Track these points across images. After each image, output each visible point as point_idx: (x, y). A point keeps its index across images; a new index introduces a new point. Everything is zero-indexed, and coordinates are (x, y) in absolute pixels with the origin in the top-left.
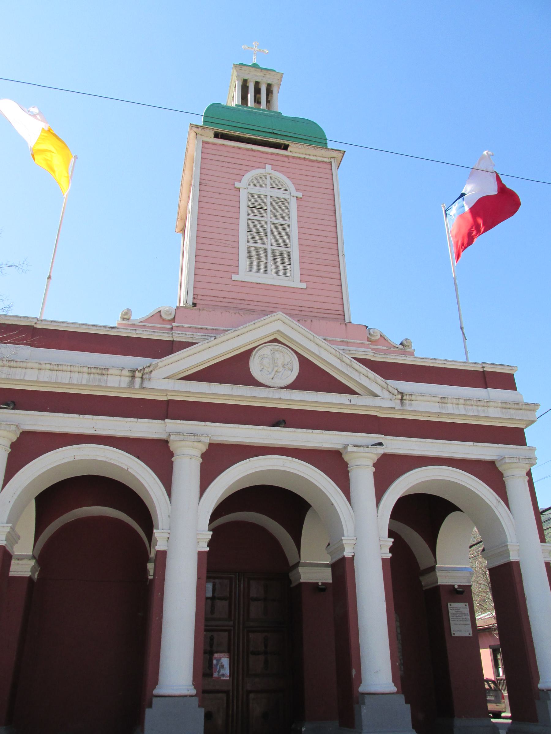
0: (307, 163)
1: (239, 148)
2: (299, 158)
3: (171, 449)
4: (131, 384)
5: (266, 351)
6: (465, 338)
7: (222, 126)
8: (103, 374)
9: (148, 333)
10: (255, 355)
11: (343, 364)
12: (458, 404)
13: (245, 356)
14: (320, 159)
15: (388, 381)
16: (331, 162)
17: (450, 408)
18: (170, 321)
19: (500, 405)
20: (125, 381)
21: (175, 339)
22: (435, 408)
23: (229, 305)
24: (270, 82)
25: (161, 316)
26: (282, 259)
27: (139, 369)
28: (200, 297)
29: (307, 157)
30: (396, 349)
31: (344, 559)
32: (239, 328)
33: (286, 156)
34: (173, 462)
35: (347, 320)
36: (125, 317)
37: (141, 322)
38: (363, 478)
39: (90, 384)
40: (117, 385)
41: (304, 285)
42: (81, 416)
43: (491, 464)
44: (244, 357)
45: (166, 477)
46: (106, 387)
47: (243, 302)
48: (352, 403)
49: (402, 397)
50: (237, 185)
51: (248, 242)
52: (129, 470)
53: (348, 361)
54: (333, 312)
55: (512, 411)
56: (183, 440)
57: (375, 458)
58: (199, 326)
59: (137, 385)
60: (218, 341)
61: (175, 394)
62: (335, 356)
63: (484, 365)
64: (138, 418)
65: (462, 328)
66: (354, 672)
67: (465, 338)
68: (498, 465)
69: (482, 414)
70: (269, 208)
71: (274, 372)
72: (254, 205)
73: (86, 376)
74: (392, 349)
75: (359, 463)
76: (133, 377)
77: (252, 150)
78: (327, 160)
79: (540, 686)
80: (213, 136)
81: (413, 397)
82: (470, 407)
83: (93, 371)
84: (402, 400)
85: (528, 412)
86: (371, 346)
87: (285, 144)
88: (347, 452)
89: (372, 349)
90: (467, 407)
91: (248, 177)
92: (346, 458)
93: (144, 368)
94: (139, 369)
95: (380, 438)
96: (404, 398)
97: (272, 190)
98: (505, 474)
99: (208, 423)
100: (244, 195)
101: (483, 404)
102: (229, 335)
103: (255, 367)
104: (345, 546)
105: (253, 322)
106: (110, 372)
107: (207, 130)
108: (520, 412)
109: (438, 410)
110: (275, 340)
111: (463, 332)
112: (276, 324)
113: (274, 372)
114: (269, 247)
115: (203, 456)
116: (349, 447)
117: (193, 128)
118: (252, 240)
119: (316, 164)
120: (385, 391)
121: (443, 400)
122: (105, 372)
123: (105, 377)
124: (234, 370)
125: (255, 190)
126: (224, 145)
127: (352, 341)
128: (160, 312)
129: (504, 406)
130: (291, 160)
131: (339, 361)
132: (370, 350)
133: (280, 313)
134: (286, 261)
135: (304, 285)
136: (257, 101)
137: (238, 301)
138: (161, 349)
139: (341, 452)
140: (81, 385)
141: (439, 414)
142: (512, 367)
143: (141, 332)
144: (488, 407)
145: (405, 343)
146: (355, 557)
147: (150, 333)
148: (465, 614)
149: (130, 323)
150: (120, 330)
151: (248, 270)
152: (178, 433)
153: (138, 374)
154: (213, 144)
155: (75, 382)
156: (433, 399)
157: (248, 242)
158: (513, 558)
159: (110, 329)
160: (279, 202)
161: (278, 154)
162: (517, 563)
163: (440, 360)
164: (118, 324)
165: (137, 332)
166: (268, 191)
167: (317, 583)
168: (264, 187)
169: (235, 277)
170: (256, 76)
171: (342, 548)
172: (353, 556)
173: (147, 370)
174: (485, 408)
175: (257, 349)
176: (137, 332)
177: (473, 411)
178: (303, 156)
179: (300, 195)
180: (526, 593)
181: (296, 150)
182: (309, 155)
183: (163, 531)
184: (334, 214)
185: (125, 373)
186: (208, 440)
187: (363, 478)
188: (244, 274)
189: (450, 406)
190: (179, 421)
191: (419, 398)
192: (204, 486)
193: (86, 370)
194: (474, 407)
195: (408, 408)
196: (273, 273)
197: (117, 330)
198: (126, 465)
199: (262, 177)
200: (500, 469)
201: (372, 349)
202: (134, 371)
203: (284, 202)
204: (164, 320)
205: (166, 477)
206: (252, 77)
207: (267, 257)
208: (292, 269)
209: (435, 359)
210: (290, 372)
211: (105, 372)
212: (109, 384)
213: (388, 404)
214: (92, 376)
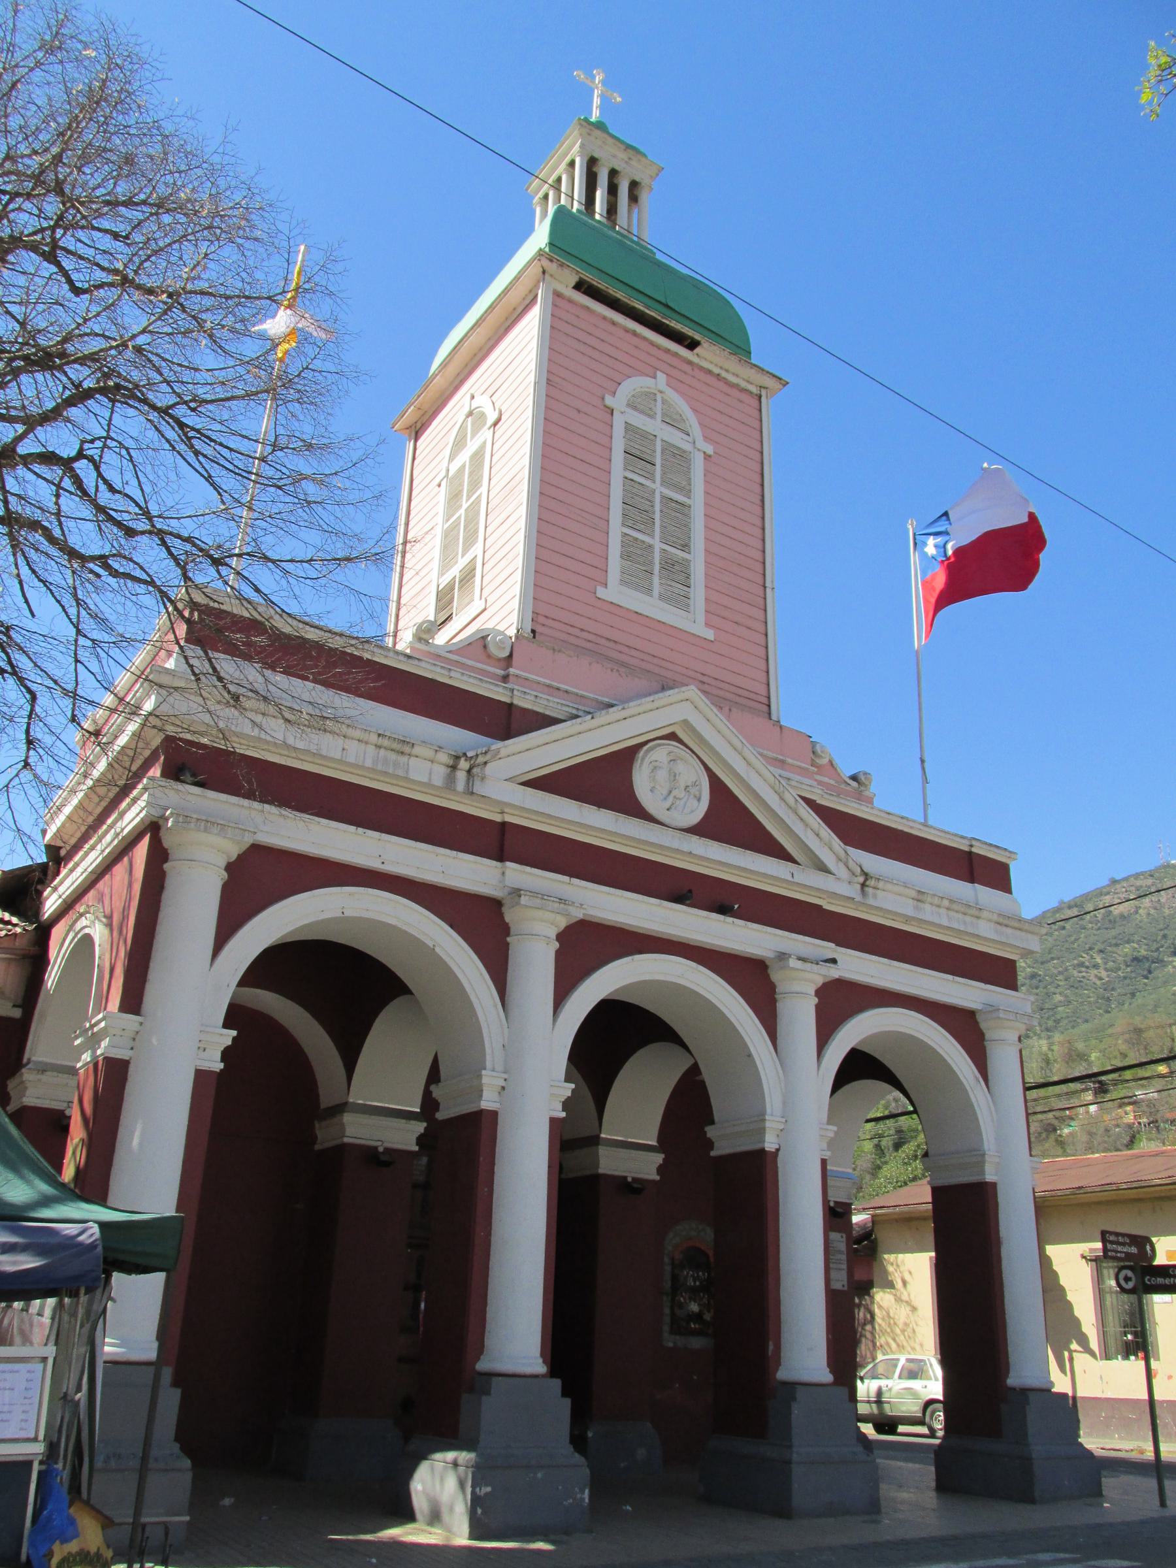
0: (721, 385)
1: (614, 323)
2: (710, 372)
3: (507, 919)
4: (450, 780)
5: (661, 754)
6: (925, 780)
7: (630, 291)
8: (402, 753)
9: (471, 680)
10: (643, 759)
11: (783, 804)
12: (939, 906)
14: (743, 384)
15: (850, 850)
16: (760, 397)
17: (928, 912)
18: (499, 660)
19: (995, 917)
20: (439, 774)
21: (515, 702)
22: (906, 907)
23: (589, 645)
24: (596, 156)
25: (485, 647)
26: (676, 571)
27: (470, 754)
28: (541, 619)
29: (724, 374)
30: (848, 788)
31: (762, 1152)
32: (631, 704)
33: (690, 363)
34: (508, 944)
35: (774, 717)
36: (424, 636)
37: (450, 652)
38: (800, 1013)
39: (380, 767)
40: (425, 780)
41: (709, 634)
42: (361, 830)
43: (970, 1015)
44: (623, 760)
46: (407, 779)
47: (611, 645)
48: (796, 879)
49: (866, 880)
50: (609, 401)
51: (623, 525)
52: (437, 950)
53: (791, 801)
54: (752, 696)
55: (1009, 931)
56: (541, 909)
57: (820, 981)
58: (555, 684)
59: (460, 785)
60: (595, 723)
61: (516, 813)
62: (773, 788)
63: (974, 843)
64: (382, 831)
65: (922, 761)
66: (771, 1347)
67: (925, 780)
68: (979, 1018)
69: (970, 930)
70: (658, 462)
72: (633, 451)
73: (371, 749)
74: (843, 786)
75: (798, 989)
76: (454, 768)
77: (635, 334)
78: (754, 390)
79: (1012, 1381)
80: (573, 284)
81: (881, 885)
82: (955, 914)
83: (386, 742)
84: (863, 885)
85: (1029, 936)
86: (818, 777)
87: (693, 339)
88: (786, 967)
89: (820, 783)
90: (951, 913)
92: (775, 976)
93: (477, 755)
94: (470, 754)
95: (828, 948)
96: (868, 883)
97: (664, 426)
98: (988, 1035)
99: (575, 881)
101: (973, 912)
102: (614, 714)
104: (767, 1131)
105: (651, 698)
106: (417, 750)
107: (566, 271)
108: (1018, 933)
109: (910, 912)
110: (672, 736)
111: (923, 769)
112: (681, 707)
114: (658, 545)
115: (560, 937)
116: (791, 960)
117: (543, 259)
118: (630, 523)
119: (735, 393)
120: (841, 865)
121: (920, 897)
122: (407, 749)
123: (405, 759)
125: (638, 420)
126: (588, 308)
127: (790, 761)
128: (484, 638)
129: (1001, 920)
130: (697, 373)
131: (776, 797)
132: (815, 783)
133: (692, 687)
134: (681, 578)
135: (709, 634)
136: (612, 210)
137: (603, 641)
138: (505, 721)
139: (768, 963)
140: (362, 767)
141: (908, 919)
142: (1011, 852)
143: (458, 676)
144: (978, 918)
145: (862, 778)
146: (780, 1153)
147: (475, 682)
148: (840, 1252)
149: (432, 650)
150: (423, 664)
151: (623, 582)
152: (534, 894)
153: (464, 765)
154: (570, 301)
155: (351, 759)
156: (907, 891)
157: (623, 525)
158: (989, 1177)
159: (405, 659)
160: (674, 455)
161: (676, 355)
162: (994, 1185)
163: (914, 821)
164: (412, 648)
165: (453, 674)
167: (625, 1178)
168: (649, 416)
169: (601, 592)
170: (614, 156)
171: (762, 1131)
172: (778, 1150)
173: (481, 759)
174: (975, 920)
175: (645, 748)
176: (453, 674)
177: (957, 921)
178: (716, 370)
179: (710, 450)
180: (1003, 1232)
181: (709, 355)
182: (727, 371)
183: (494, 1074)
184: (759, 502)
185: (443, 758)
186: (578, 915)
187: (800, 1013)
188: (614, 591)
189: (927, 907)
190: (528, 869)
191: (889, 887)
193: (373, 738)
194: (960, 916)
195: (871, 901)
196: (661, 597)
197: (416, 662)
198: (432, 939)
199: (650, 394)
200: (983, 1026)
201: (820, 783)
202: (457, 758)
204: (489, 656)
206: (610, 158)
207: (652, 563)
208: (692, 596)
209: (907, 819)
210: (695, 803)
211: (407, 749)
212: (412, 776)
213: (844, 889)
214: (382, 751)
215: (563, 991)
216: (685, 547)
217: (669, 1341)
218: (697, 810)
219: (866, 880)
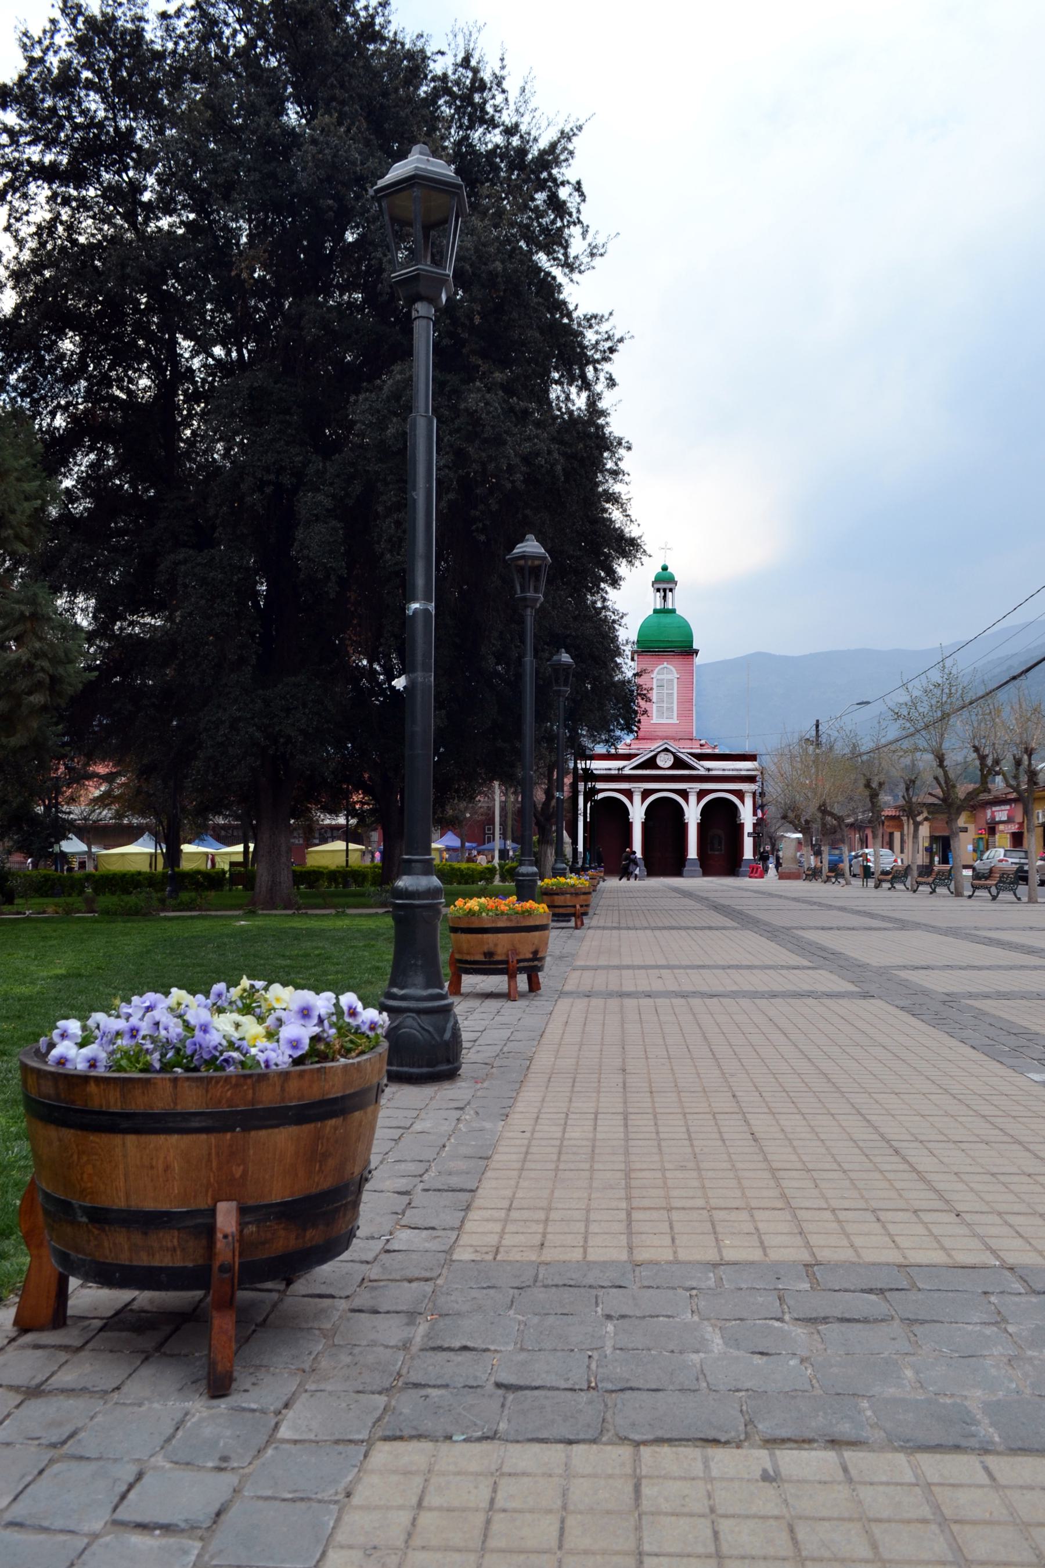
5: (662, 754)
13: (654, 757)
44: (654, 757)
71: (665, 761)
103: (660, 762)
113: (665, 761)
124: (651, 763)
125: (660, 677)
166: (665, 677)
203: (672, 680)
215: (643, 801)
218: (670, 763)
219: (709, 770)
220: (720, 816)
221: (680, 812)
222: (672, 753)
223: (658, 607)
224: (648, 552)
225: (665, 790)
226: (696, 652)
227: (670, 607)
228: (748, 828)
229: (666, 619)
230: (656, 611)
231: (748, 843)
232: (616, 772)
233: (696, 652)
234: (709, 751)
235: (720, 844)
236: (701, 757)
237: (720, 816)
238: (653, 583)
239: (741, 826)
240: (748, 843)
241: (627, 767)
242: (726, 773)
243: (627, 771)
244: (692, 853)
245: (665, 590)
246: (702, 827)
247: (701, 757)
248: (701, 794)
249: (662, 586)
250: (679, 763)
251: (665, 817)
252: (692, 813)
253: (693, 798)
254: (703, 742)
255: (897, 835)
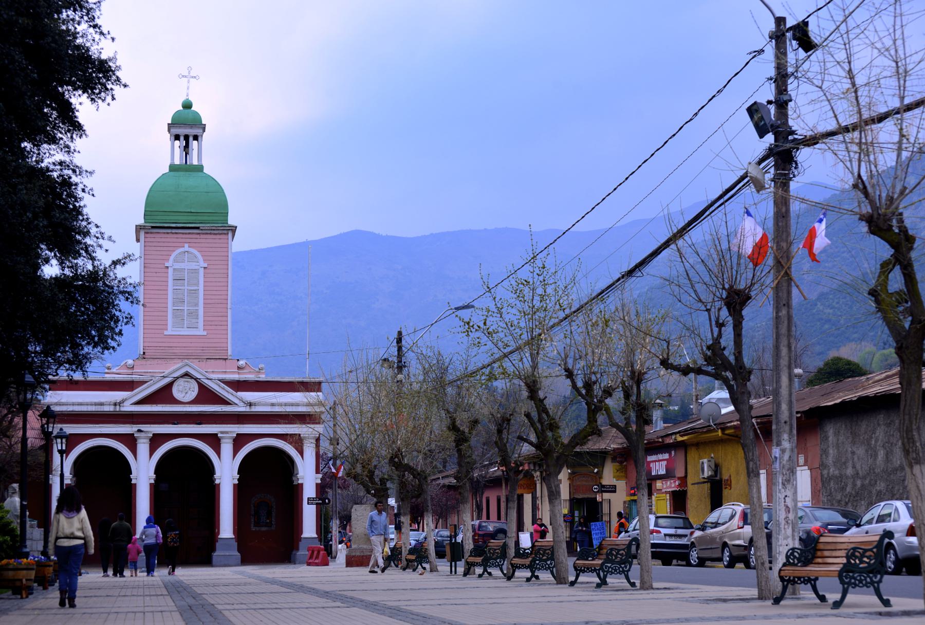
5: (181, 382)
13: (169, 386)
44: (169, 386)
45: (134, 451)
71: (185, 392)
91: (172, 258)
100: (170, 270)
113: (185, 392)
114: (186, 308)
124: (164, 394)
125: (177, 266)
162: (302, 484)
169: (166, 333)
192: (151, 454)
205: (134, 451)
215: (152, 452)
216: (197, 305)
217: (273, 528)
219: (250, 405)
220: (268, 473)
221: (209, 469)
222: (196, 379)
223: (177, 162)
224: (123, 81)
225: (185, 436)
226: (233, 229)
227: (195, 162)
228: (309, 491)
229: (188, 181)
230: (173, 168)
231: (309, 514)
232: (111, 408)
233: (233, 229)
234: (251, 377)
235: (269, 515)
236: (239, 386)
237: (268, 473)
238: (170, 126)
239: (298, 489)
240: (309, 514)
241: (128, 401)
242: (277, 409)
243: (128, 408)
244: (226, 528)
245: (186, 138)
246: (239, 490)
247: (239, 386)
248: (156, 441)
249: (182, 131)
250: (206, 395)
251: (186, 476)
252: (226, 471)
253: (227, 447)
254: (242, 363)
255: (528, 498)
